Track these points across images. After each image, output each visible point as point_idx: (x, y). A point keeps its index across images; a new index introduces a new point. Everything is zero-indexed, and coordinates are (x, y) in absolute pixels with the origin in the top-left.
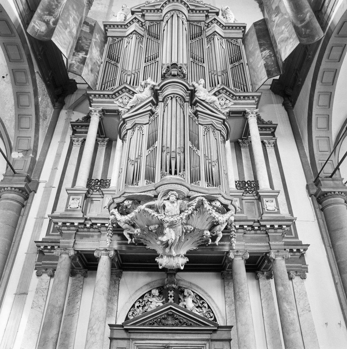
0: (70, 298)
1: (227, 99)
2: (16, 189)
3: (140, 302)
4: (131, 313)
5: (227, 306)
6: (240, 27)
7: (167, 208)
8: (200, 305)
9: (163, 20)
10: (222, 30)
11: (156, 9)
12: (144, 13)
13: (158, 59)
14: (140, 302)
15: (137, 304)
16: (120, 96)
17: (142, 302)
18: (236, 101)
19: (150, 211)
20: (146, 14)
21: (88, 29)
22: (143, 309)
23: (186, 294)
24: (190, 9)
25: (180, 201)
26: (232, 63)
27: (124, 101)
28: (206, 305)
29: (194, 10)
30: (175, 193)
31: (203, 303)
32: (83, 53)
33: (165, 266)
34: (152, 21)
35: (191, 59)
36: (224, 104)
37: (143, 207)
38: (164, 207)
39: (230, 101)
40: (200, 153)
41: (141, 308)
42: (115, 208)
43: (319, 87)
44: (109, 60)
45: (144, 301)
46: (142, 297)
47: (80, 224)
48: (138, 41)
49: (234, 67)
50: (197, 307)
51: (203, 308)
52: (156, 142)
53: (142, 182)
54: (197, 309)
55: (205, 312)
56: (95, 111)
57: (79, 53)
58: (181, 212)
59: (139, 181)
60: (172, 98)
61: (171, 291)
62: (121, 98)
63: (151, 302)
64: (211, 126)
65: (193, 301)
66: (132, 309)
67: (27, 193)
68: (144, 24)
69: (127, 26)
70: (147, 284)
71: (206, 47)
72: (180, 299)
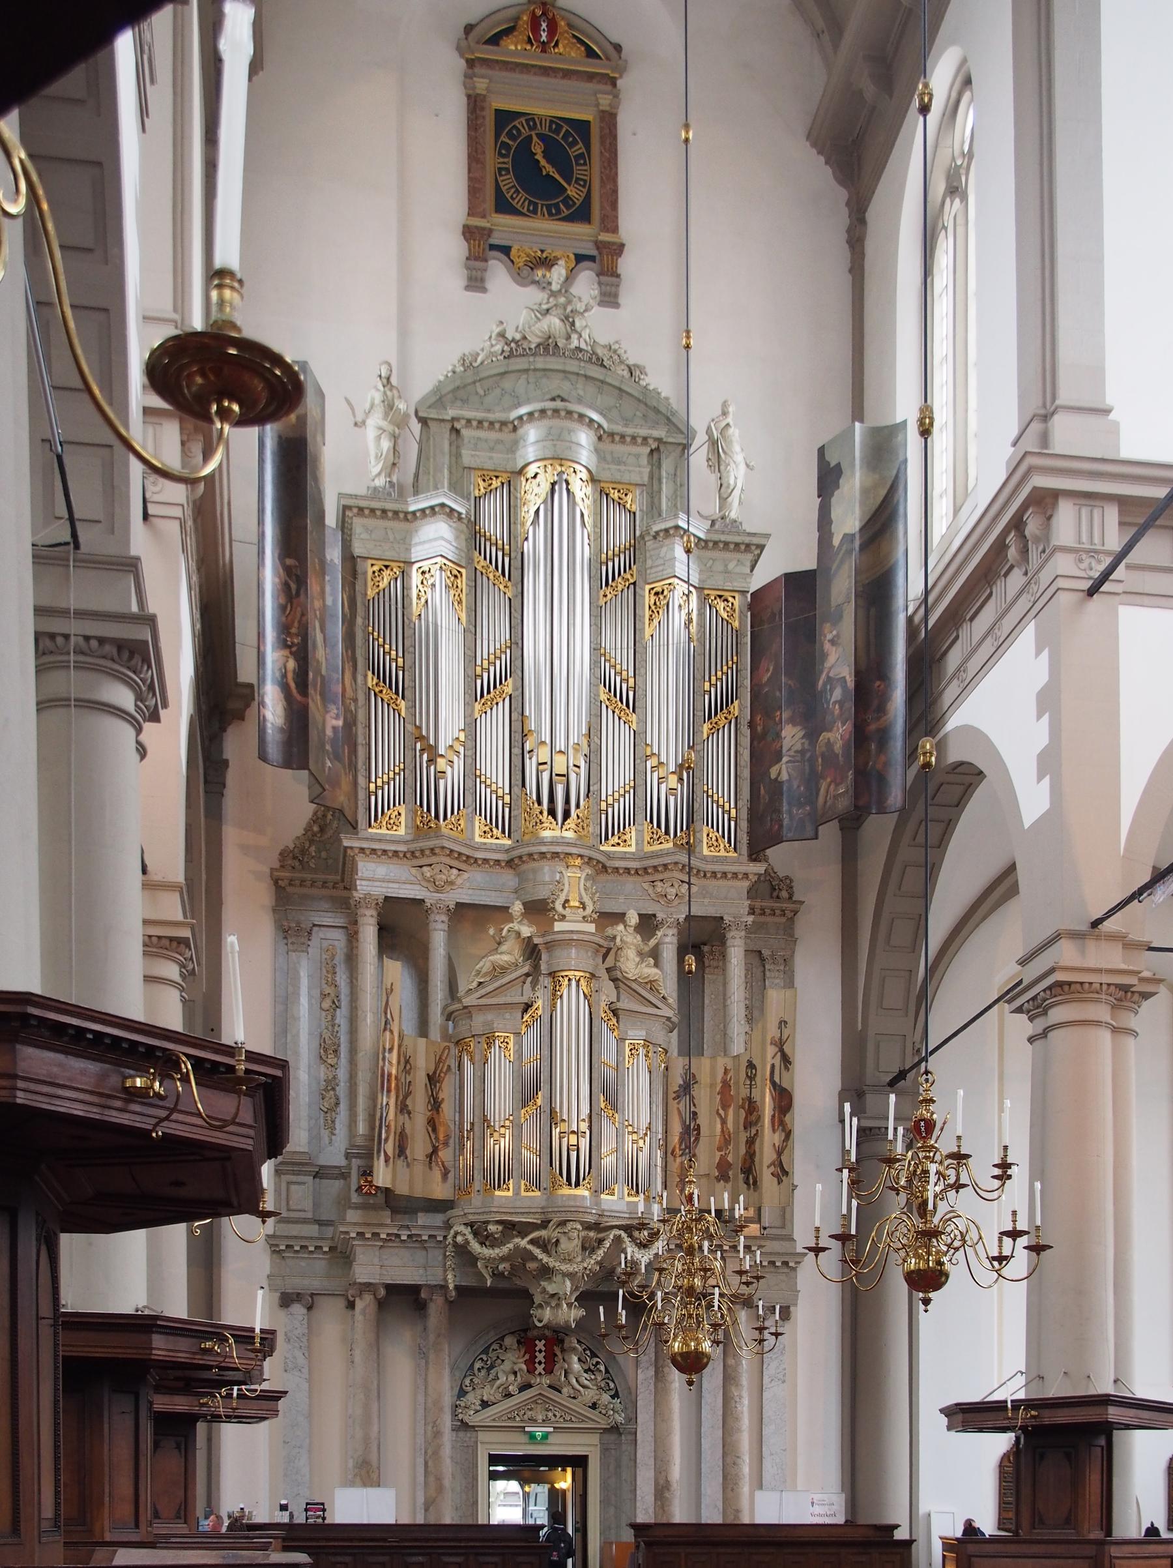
5: (639, 1371)
19: (537, 1252)
37: (523, 1243)
52: (539, 1093)
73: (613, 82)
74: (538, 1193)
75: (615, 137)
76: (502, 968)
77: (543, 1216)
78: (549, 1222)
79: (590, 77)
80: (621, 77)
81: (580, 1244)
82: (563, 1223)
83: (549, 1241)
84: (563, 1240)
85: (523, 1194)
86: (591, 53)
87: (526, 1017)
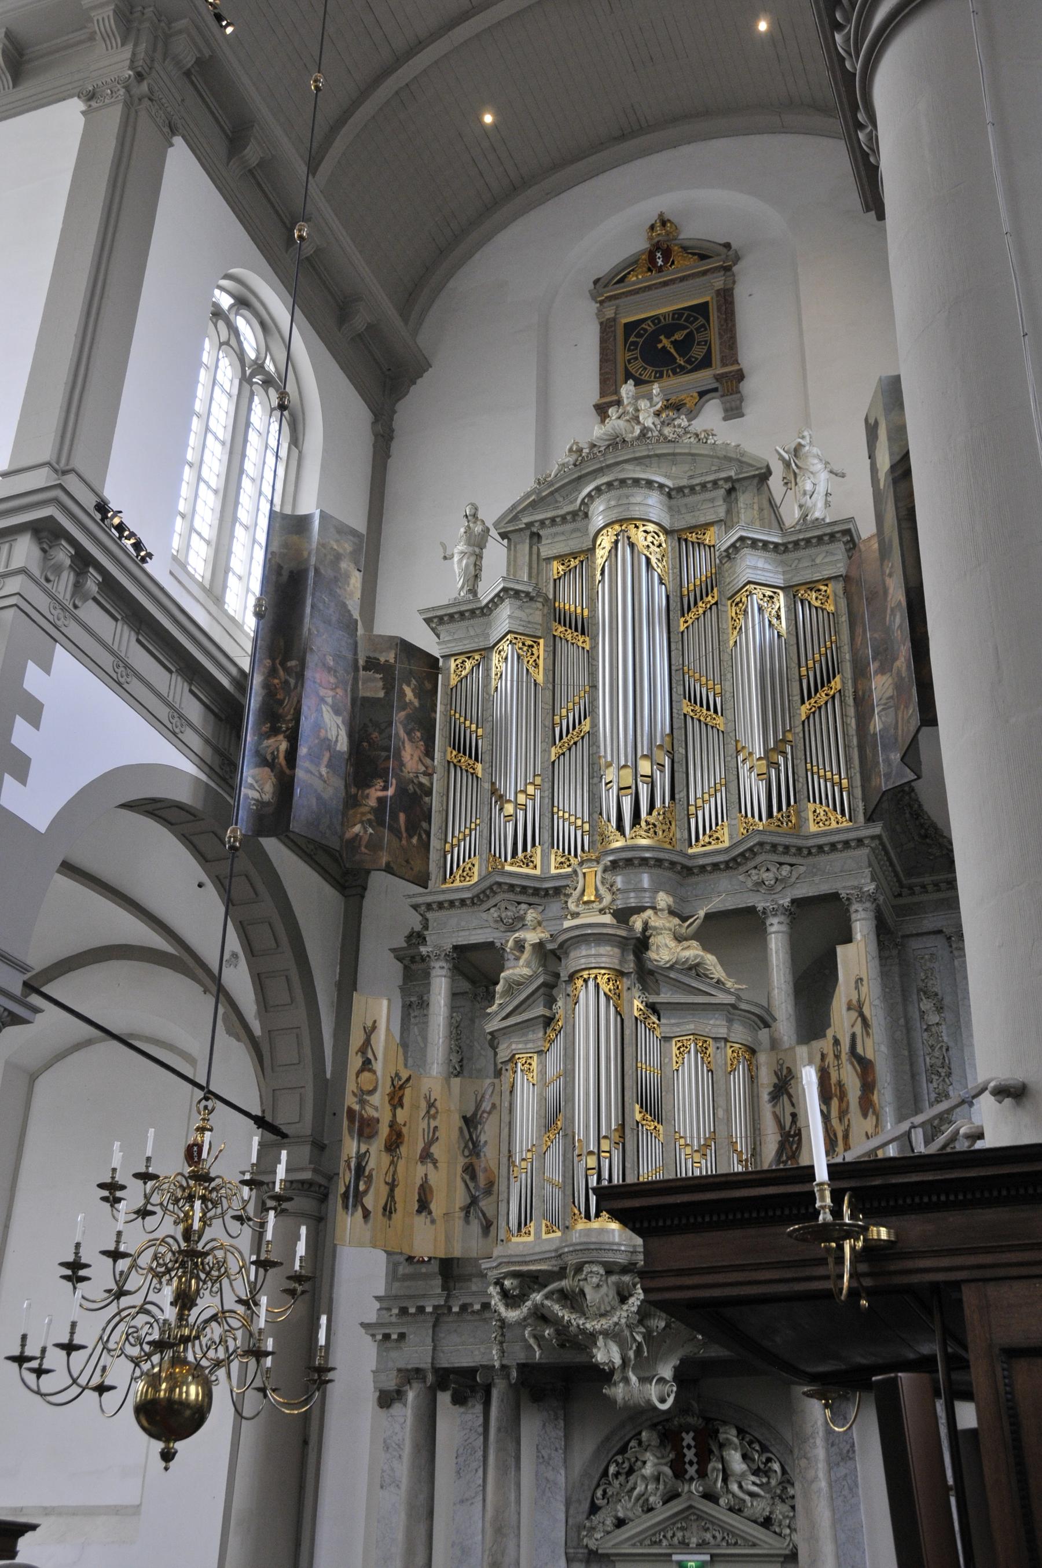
0: (459, 1460)
1: (781, 864)
2: (294, 1185)
3: (616, 1461)
4: (599, 1493)
6: (832, 536)
7: (588, 1297)
8: (762, 1466)
9: (592, 550)
10: (779, 557)
11: (568, 513)
12: (535, 530)
14: (618, 1464)
15: (612, 1469)
16: (492, 902)
17: (623, 1462)
18: (811, 860)
20: (541, 533)
21: (381, 684)
23: (722, 1437)
24: (671, 489)
25: (613, 1278)
26: (809, 697)
27: (503, 915)
28: (776, 1466)
29: (684, 487)
30: (595, 1269)
31: (769, 1460)
32: (378, 787)
33: (625, 1402)
36: (772, 882)
37: (538, 1297)
38: (582, 1293)
39: (792, 865)
41: (622, 1478)
44: (454, 753)
45: (629, 1459)
47: (435, 1307)
49: (814, 713)
50: (756, 1472)
51: (772, 1475)
54: (753, 1478)
55: (773, 1482)
56: (438, 956)
57: (367, 791)
58: (623, 1299)
59: (532, 1224)
60: (586, 981)
61: (688, 1433)
62: (495, 906)
63: (644, 1463)
64: (691, 1037)
65: (745, 1457)
66: (603, 1481)
67: (320, 1186)
68: (533, 594)
69: (486, 611)
72: (711, 1452)
73: (727, 269)
74: (559, 1234)
75: (732, 303)
76: (519, 984)
77: (560, 1262)
78: (566, 1268)
79: (704, 273)
80: (735, 264)
81: (612, 1293)
82: (579, 1269)
83: (573, 1291)
84: (588, 1290)
85: (544, 1236)
86: (703, 257)
87: (548, 1031)
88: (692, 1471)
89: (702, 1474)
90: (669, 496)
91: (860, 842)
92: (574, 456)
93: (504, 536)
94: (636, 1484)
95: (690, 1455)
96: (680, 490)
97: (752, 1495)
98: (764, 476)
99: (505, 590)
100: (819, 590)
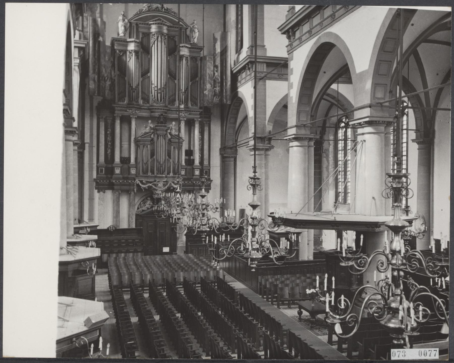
12: (138, 24)
13: (149, 75)
15: (142, 203)
19: (153, 186)
20: (140, 25)
22: (144, 204)
34: (143, 33)
35: (168, 76)
37: (151, 185)
38: (158, 184)
40: (171, 161)
42: (139, 180)
43: (232, 107)
46: (144, 200)
48: (136, 57)
53: (150, 174)
60: (161, 136)
70: (145, 195)
71: (178, 64)
88: (155, 203)
89: (157, 204)
90: (168, 27)
91: (199, 111)
92: (147, 8)
93: (130, 23)
94: (146, 205)
95: (155, 201)
96: (171, 27)
97: (165, 207)
98: (187, 28)
99: (134, 41)
100: (195, 58)
